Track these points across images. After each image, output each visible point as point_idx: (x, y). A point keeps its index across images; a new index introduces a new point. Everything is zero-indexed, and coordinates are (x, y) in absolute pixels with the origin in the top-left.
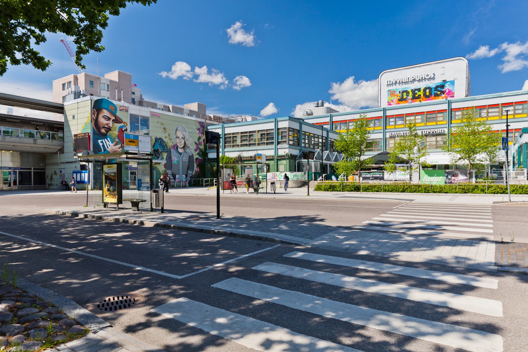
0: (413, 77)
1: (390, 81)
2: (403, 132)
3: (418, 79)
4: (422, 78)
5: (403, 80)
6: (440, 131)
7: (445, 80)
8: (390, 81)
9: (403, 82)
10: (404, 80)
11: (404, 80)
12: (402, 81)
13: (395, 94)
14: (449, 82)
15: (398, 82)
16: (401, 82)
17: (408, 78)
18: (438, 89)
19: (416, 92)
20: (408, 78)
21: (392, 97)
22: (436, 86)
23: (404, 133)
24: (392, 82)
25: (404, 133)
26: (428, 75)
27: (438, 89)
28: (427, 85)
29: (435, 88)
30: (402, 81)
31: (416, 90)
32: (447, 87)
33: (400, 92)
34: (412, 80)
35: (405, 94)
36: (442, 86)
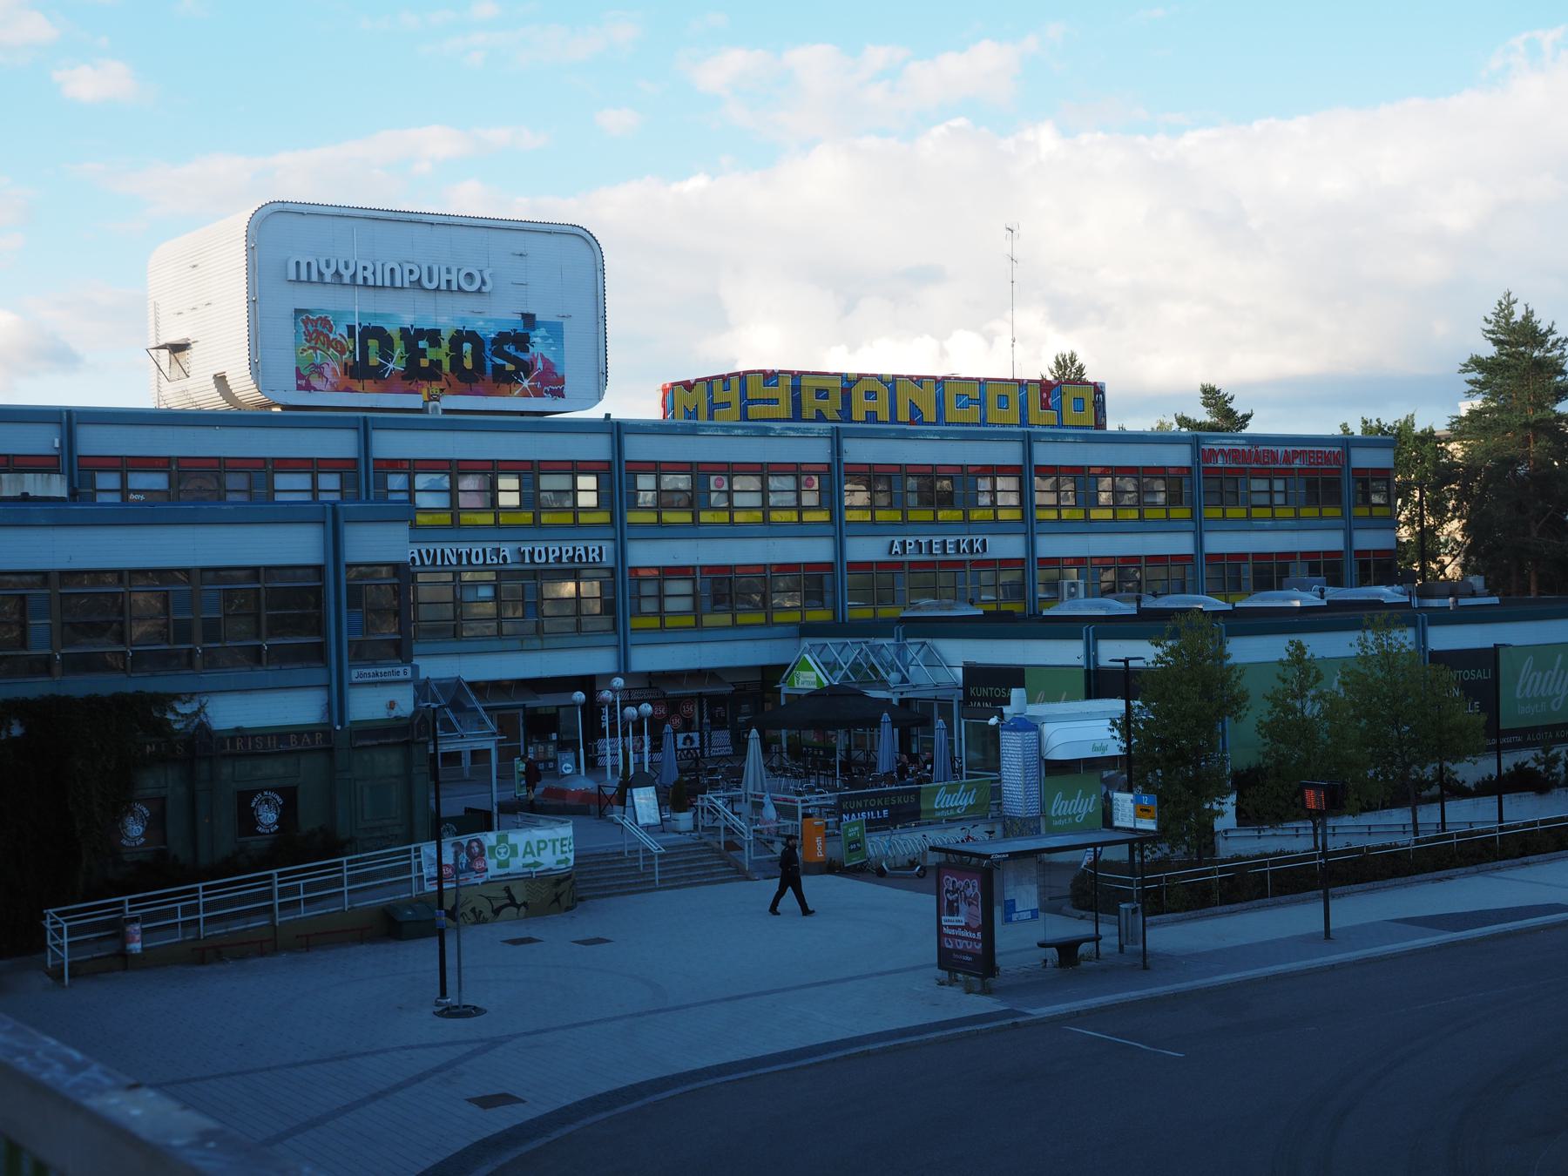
0: (411, 272)
1: (309, 264)
2: (454, 546)
3: (434, 285)
4: (449, 282)
5: (368, 274)
6: (595, 555)
7: (531, 311)
8: (309, 264)
9: (371, 282)
10: (374, 273)
11: (374, 273)
12: (365, 279)
13: (332, 336)
14: (544, 324)
15: (347, 280)
16: (360, 281)
17: (392, 270)
18: (506, 347)
19: (422, 344)
20: (392, 270)
21: (315, 349)
22: (500, 334)
23: (459, 556)
24: (320, 274)
25: (459, 556)
26: (469, 275)
27: (506, 347)
28: (462, 319)
29: (494, 341)
30: (365, 279)
31: (421, 334)
32: (539, 346)
33: (351, 329)
34: (407, 284)
35: (373, 344)
36: (522, 341)
